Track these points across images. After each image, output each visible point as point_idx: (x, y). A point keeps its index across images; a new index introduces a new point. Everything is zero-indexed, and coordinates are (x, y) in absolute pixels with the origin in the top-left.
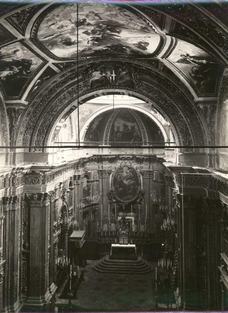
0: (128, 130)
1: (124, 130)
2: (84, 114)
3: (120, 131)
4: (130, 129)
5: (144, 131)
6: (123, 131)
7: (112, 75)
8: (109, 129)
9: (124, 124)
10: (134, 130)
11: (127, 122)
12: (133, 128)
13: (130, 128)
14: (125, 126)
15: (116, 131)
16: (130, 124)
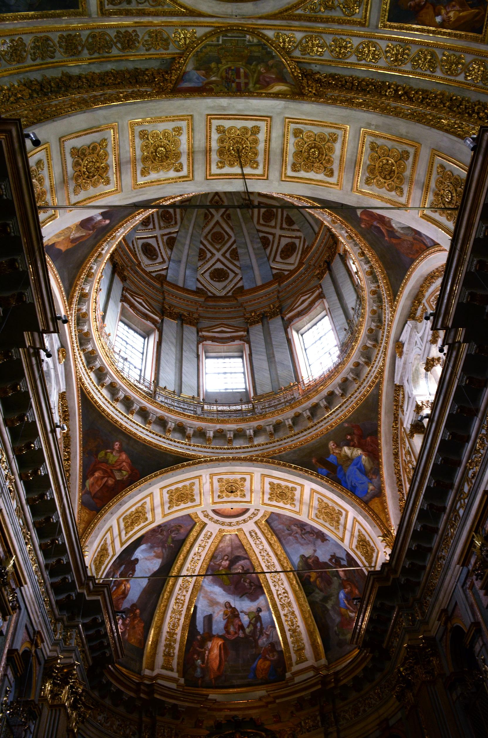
0: (241, 627)
1: (226, 627)
2: (111, 475)
3: (214, 633)
4: (245, 626)
5: (293, 613)
6: (224, 632)
7: (237, 80)
8: (180, 614)
9: (228, 605)
10: (259, 624)
11: (237, 598)
12: (256, 617)
13: (245, 619)
14: (232, 614)
15: (201, 633)
16: (244, 606)
